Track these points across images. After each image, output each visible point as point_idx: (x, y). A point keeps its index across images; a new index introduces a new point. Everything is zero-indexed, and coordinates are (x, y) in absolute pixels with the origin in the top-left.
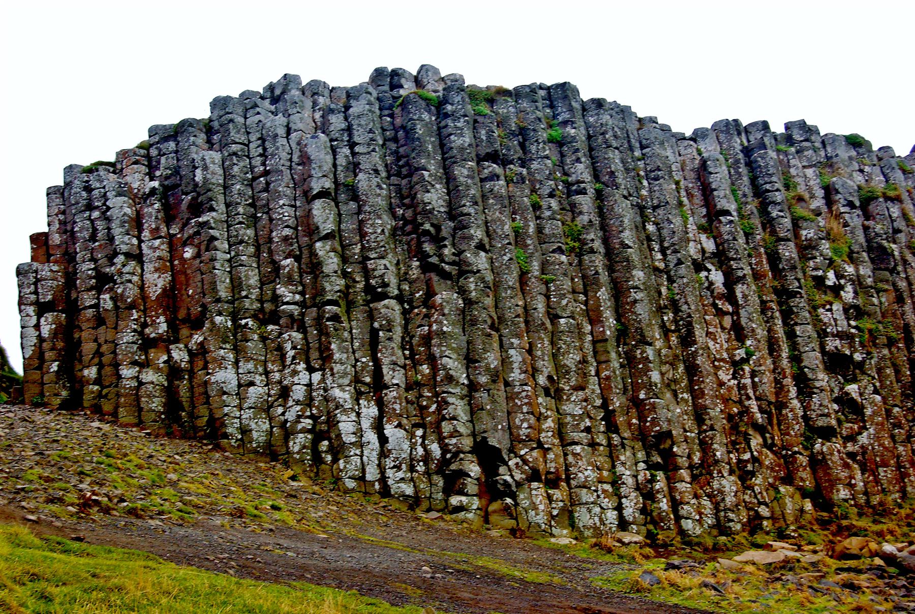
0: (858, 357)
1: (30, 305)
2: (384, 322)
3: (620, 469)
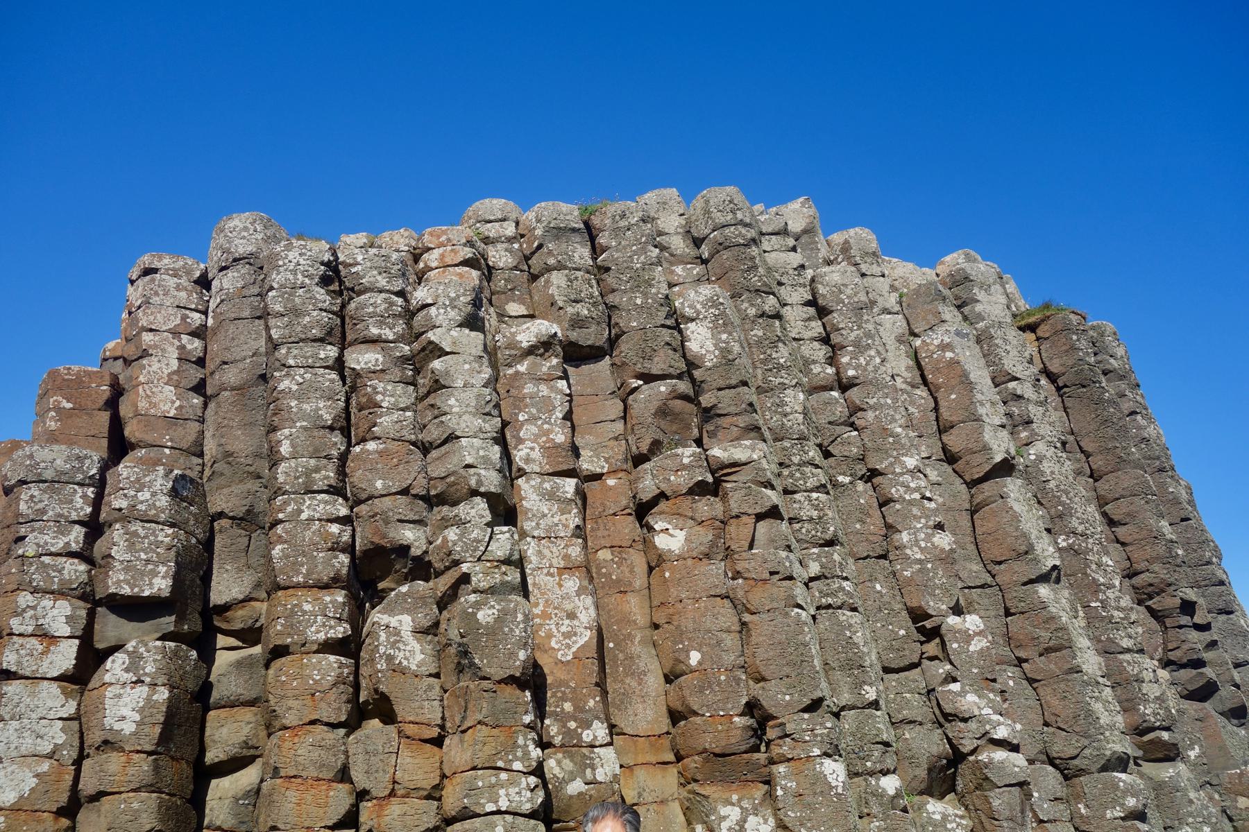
1: (60, 594)
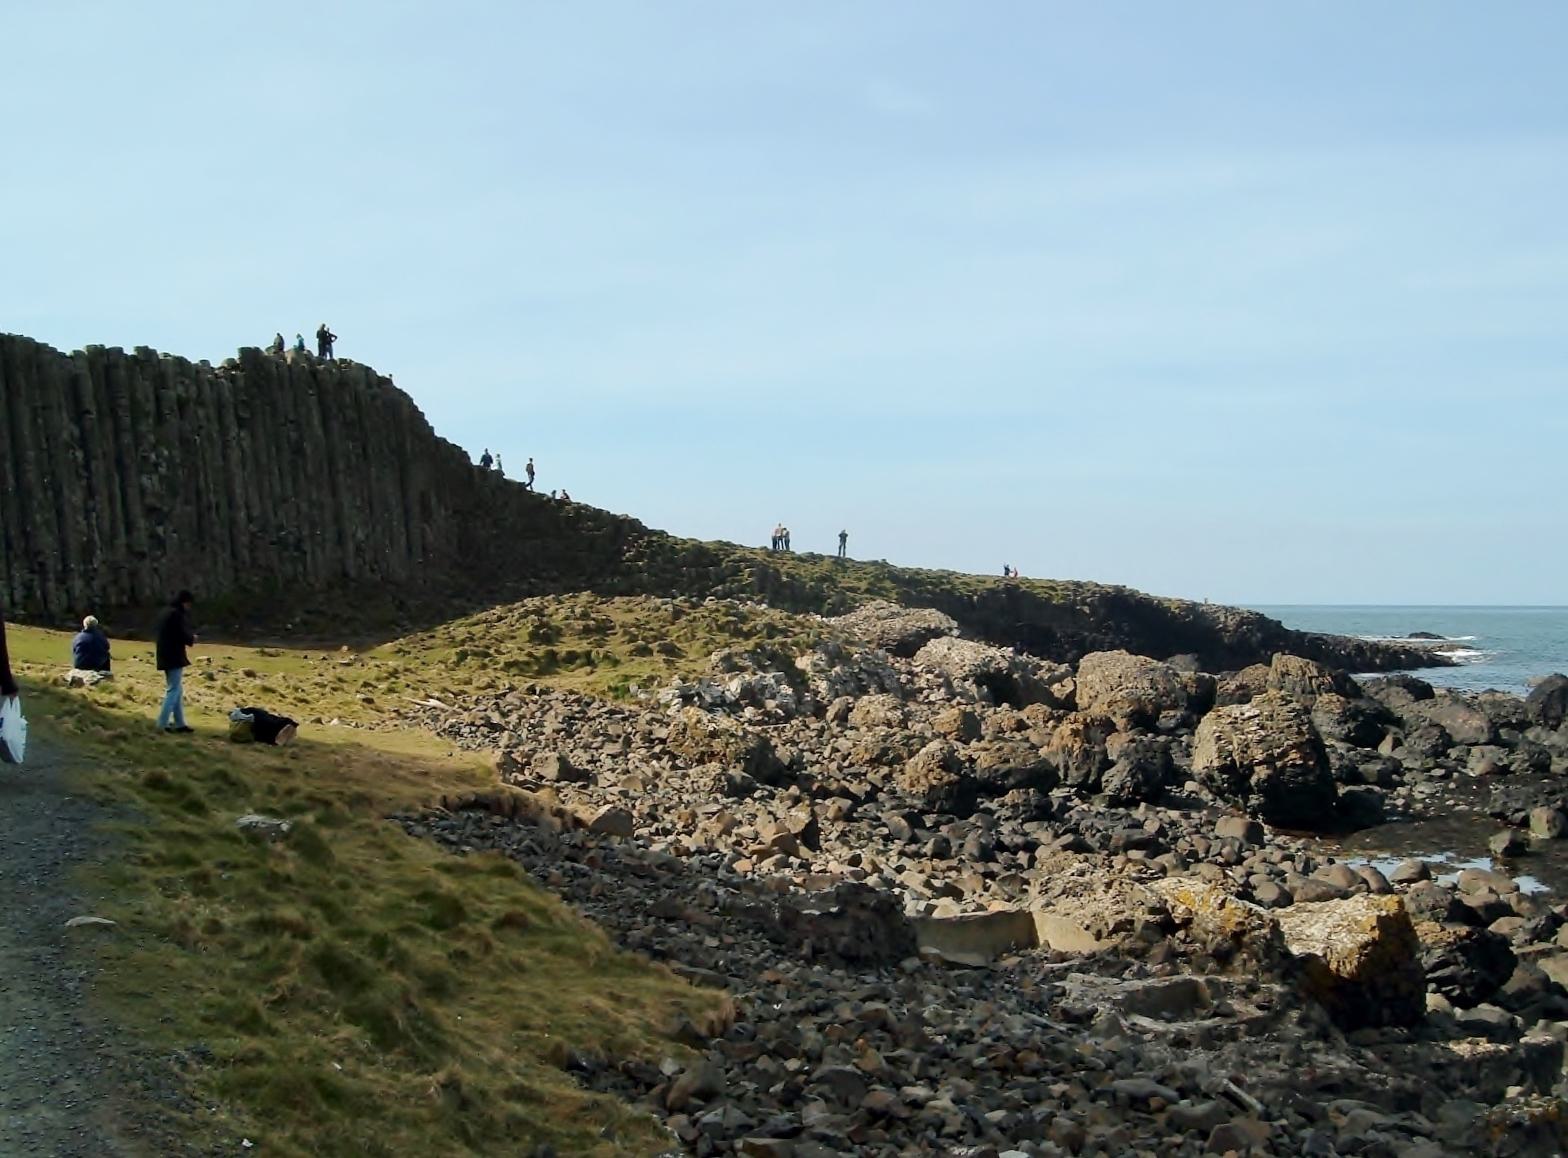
0: (166, 509)
3: (13, 572)
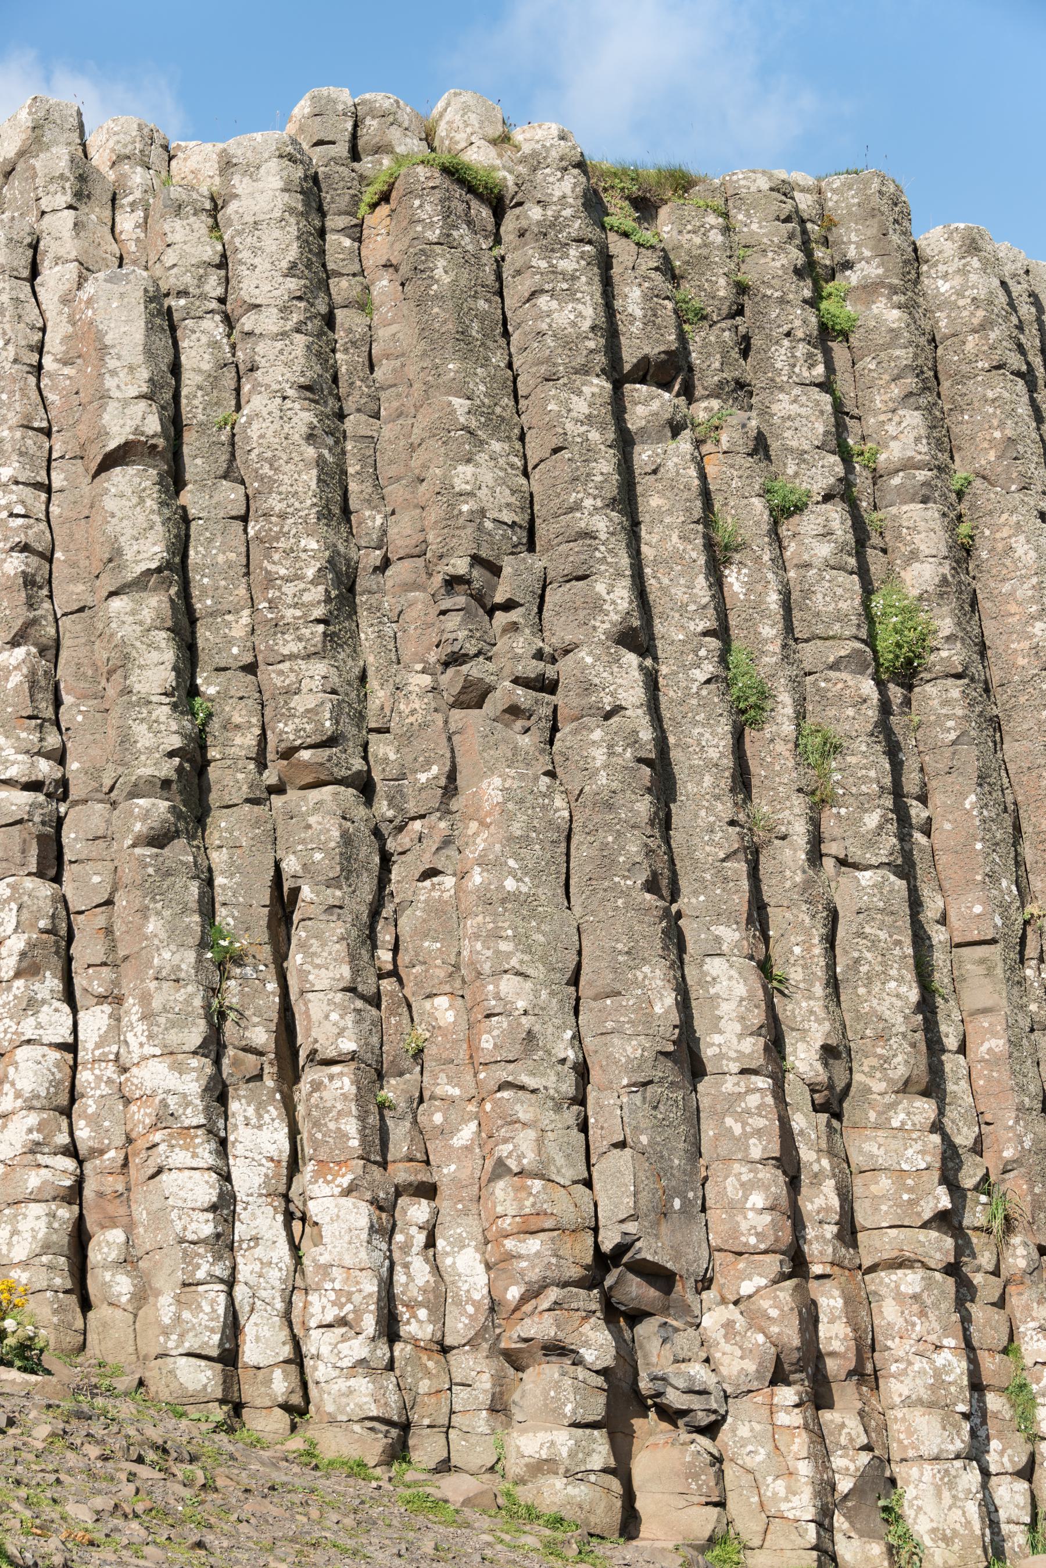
2: (318, 856)
